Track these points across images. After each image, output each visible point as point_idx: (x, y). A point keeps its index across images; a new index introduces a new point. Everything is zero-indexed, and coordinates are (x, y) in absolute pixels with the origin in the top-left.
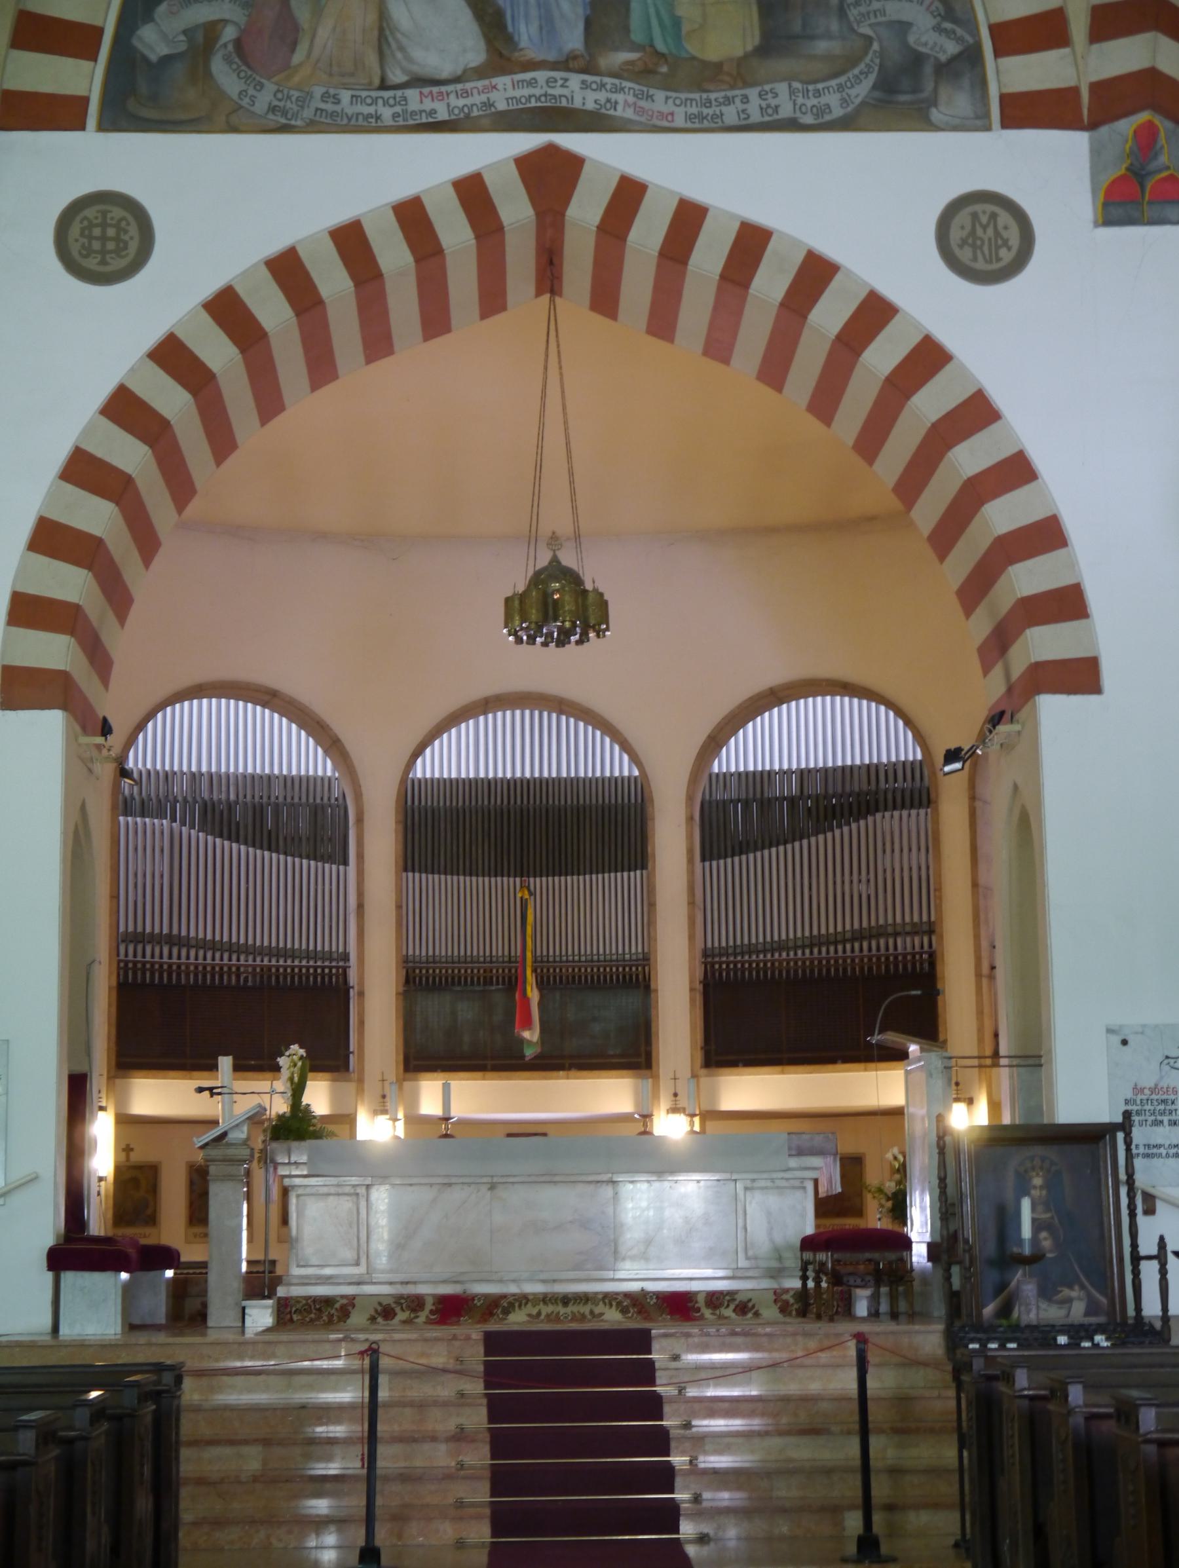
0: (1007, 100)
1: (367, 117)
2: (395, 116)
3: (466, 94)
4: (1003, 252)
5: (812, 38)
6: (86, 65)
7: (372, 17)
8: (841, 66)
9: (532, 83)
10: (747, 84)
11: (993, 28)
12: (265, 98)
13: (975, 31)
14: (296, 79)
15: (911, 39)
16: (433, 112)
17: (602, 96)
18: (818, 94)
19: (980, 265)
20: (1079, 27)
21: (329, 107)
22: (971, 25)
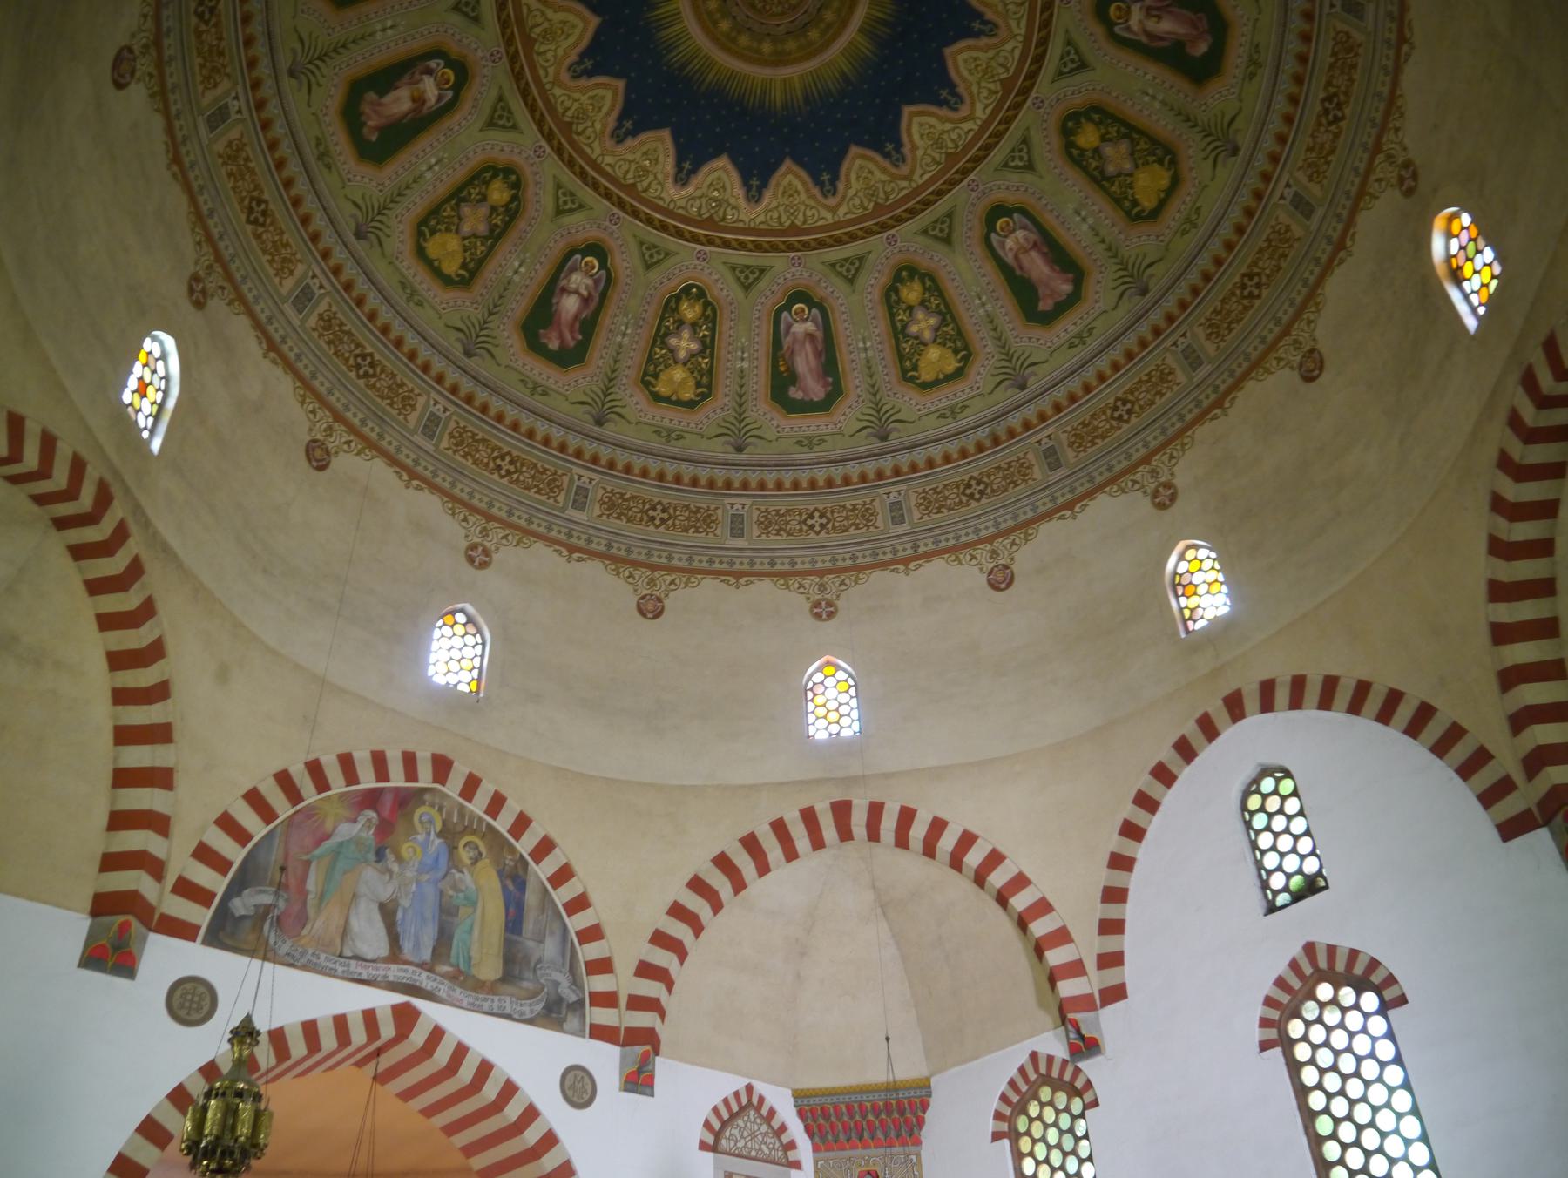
0: (592, 1026)
1: (331, 969)
2: (343, 972)
3: (377, 969)
4: (584, 1095)
5: (522, 979)
6: (203, 909)
7: (342, 922)
8: (532, 995)
9: (406, 971)
10: (495, 994)
11: (590, 993)
12: (285, 948)
13: (584, 994)
14: (303, 942)
15: (559, 990)
16: (360, 974)
17: (435, 984)
18: (521, 1005)
19: (575, 1099)
20: (623, 1001)
21: (315, 960)
22: (582, 988)
